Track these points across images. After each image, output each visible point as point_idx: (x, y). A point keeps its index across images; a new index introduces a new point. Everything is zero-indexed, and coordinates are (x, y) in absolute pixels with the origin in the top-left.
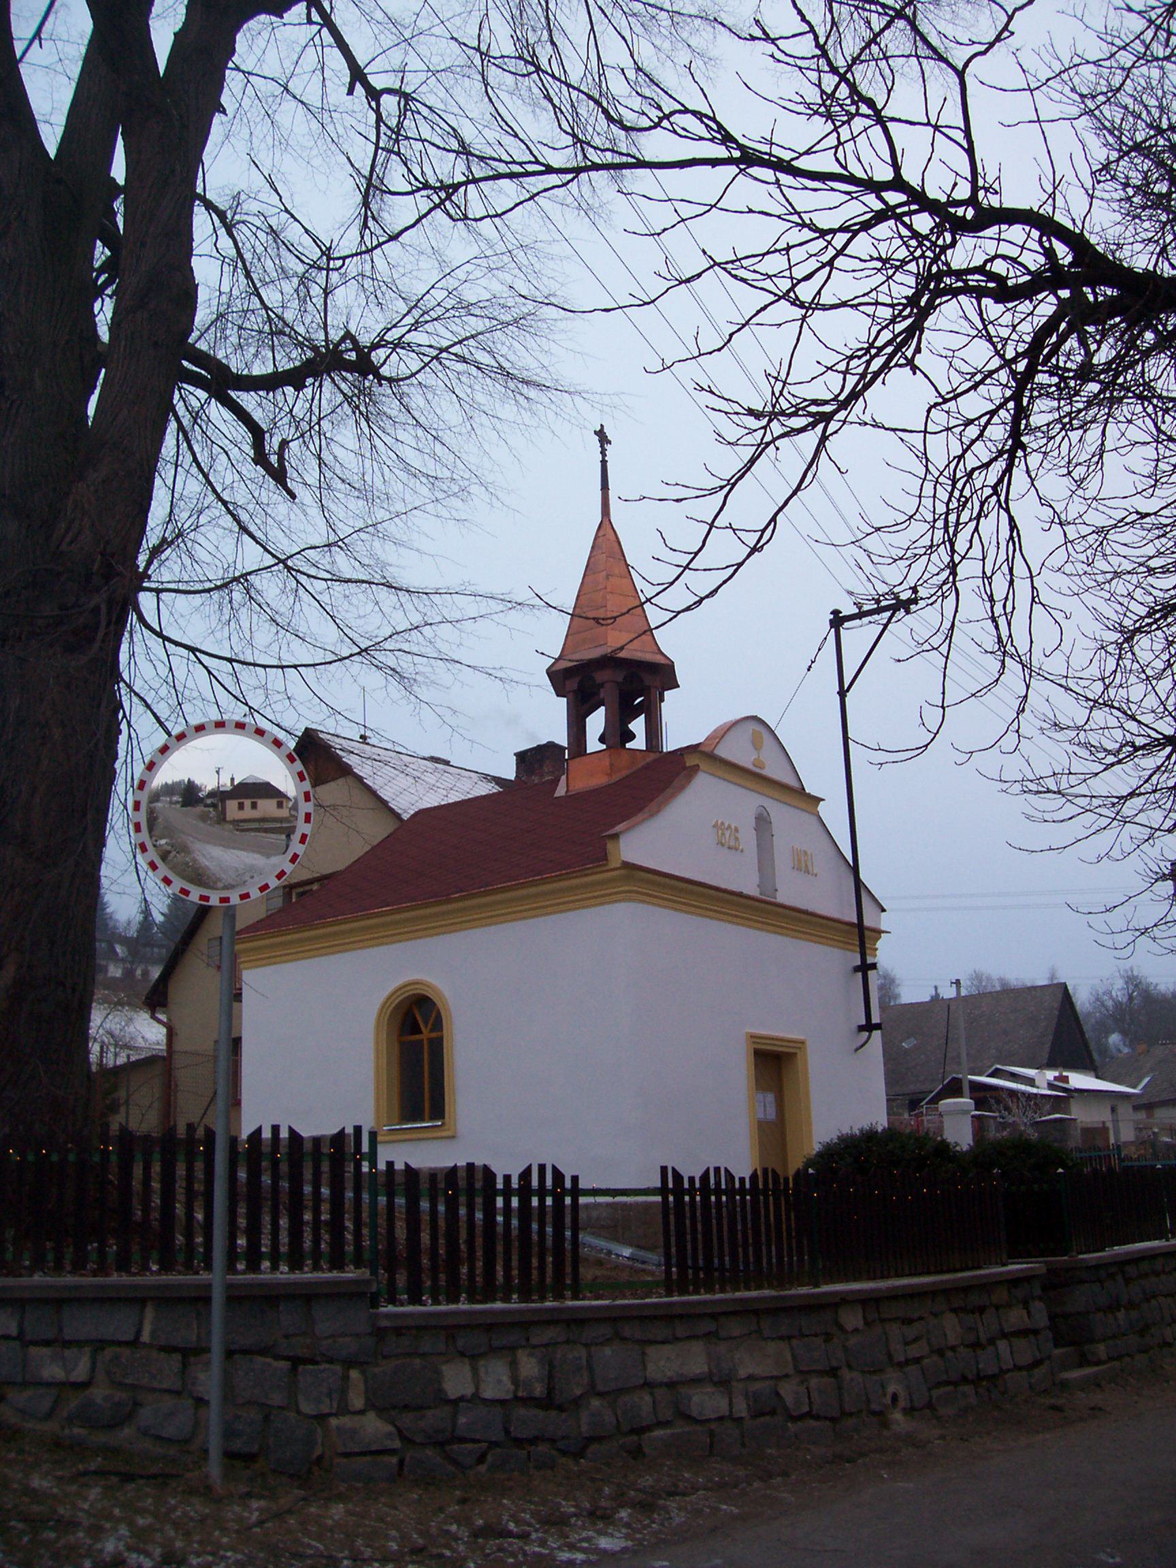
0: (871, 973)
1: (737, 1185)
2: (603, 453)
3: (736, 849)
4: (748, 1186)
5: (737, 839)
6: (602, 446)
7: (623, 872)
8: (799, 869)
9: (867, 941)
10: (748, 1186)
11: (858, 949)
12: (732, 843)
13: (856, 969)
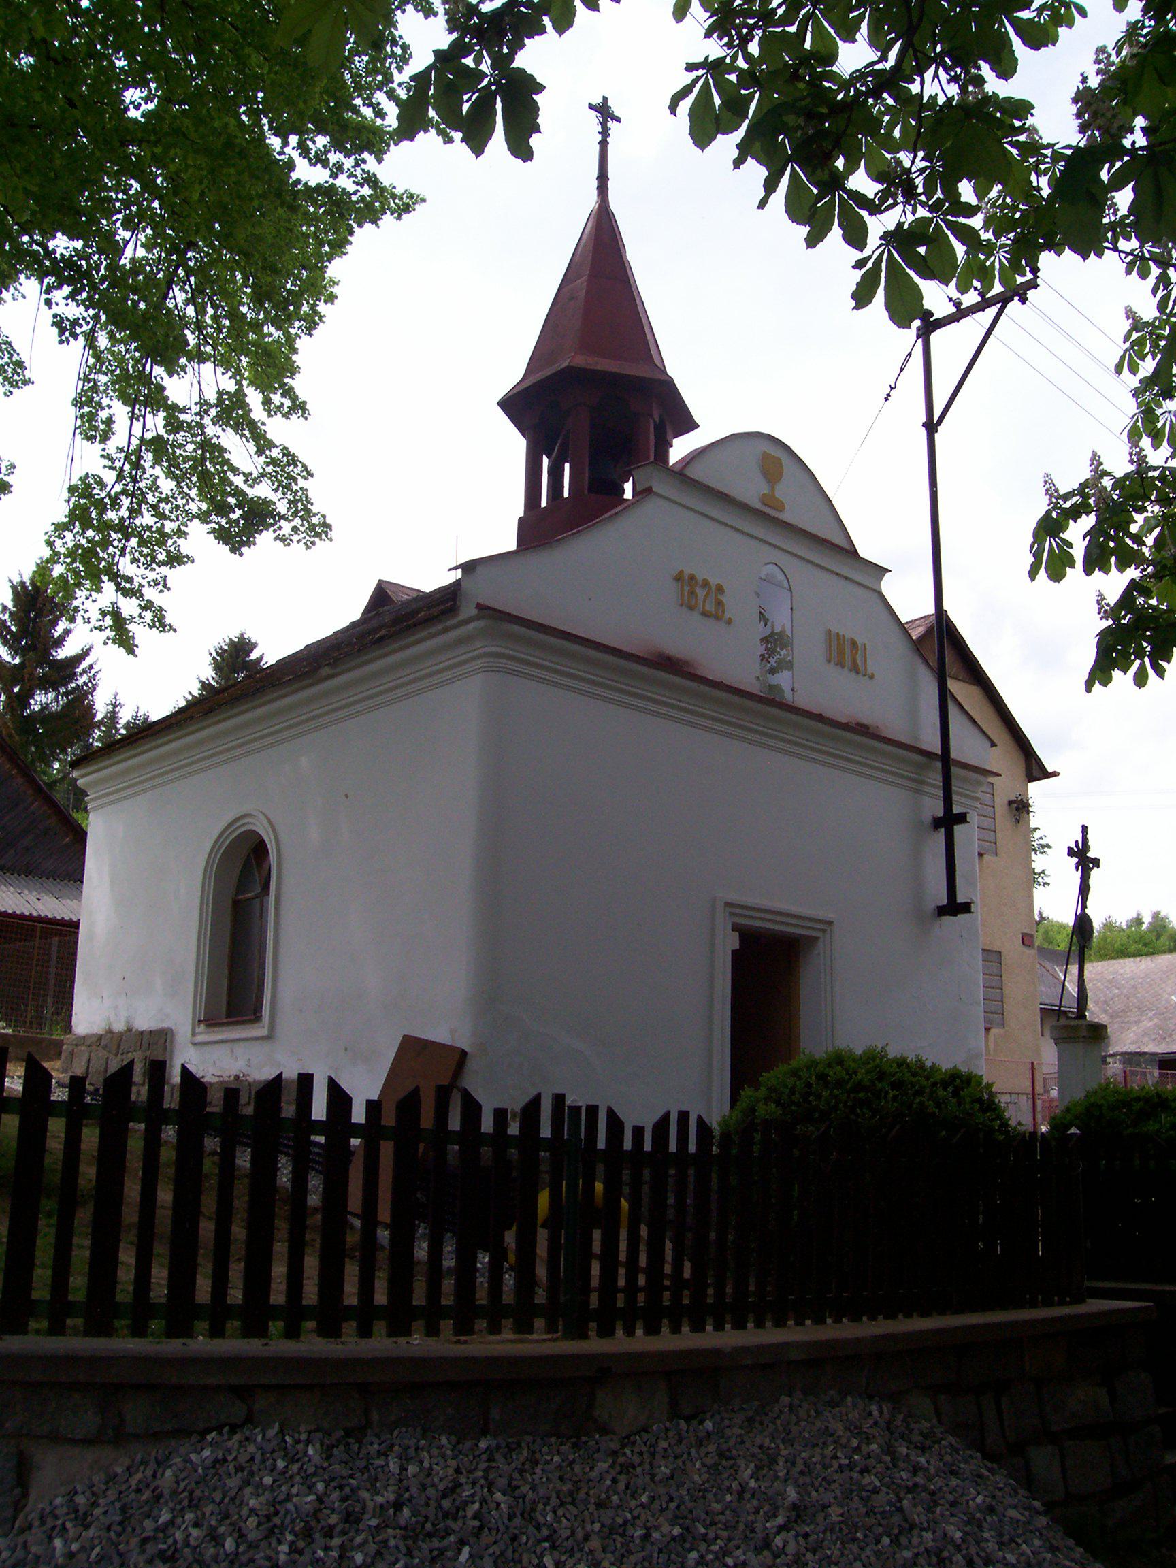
0: (958, 829)
1: (628, 1145)
2: (605, 133)
3: (718, 618)
4: (648, 1146)
5: (719, 603)
6: (604, 125)
7: (481, 624)
8: (841, 664)
9: (954, 782)
10: (648, 1146)
11: (941, 793)
12: (710, 607)
13: (937, 823)
